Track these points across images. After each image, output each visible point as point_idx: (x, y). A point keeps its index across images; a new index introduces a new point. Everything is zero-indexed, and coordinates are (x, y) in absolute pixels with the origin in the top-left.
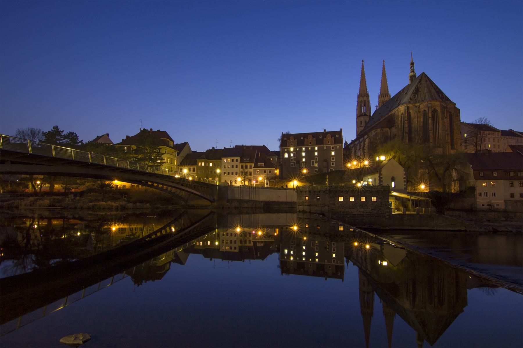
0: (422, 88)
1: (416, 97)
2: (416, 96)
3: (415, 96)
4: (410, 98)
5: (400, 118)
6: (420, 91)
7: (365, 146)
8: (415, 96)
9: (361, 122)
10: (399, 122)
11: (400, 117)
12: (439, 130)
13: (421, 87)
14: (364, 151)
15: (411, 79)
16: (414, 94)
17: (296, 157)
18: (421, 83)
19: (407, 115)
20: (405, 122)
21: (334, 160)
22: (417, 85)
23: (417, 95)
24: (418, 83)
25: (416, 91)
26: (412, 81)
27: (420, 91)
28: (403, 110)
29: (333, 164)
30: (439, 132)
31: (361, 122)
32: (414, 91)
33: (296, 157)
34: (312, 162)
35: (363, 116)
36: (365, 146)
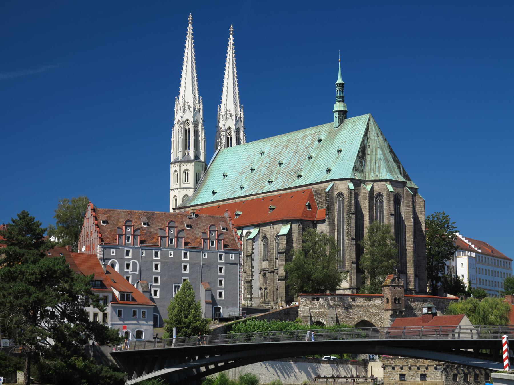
0: (371, 147)
1: (363, 165)
2: (363, 162)
3: (362, 162)
4: (355, 166)
5: (335, 205)
6: (368, 154)
7: (253, 251)
8: (361, 162)
9: (186, 175)
10: (335, 210)
11: (335, 201)
12: (402, 239)
13: (369, 145)
14: (252, 264)
15: (338, 116)
16: (360, 158)
17: (137, 273)
18: (368, 136)
19: (353, 202)
20: (351, 215)
21: (224, 287)
22: (363, 141)
23: (365, 162)
24: (364, 136)
25: (362, 153)
26: (340, 120)
27: (368, 154)
28: (344, 189)
29: (220, 294)
30: (402, 242)
31: (186, 175)
32: (359, 152)
33: (137, 273)
34: (175, 287)
35: (191, 162)
36: (253, 251)
